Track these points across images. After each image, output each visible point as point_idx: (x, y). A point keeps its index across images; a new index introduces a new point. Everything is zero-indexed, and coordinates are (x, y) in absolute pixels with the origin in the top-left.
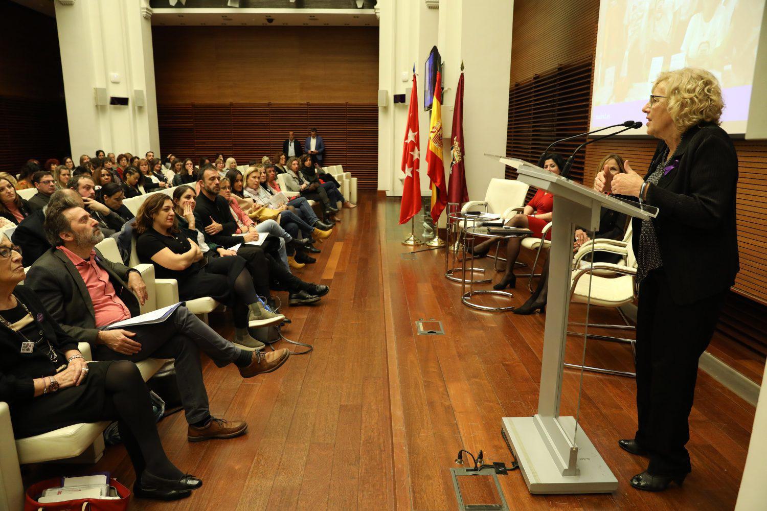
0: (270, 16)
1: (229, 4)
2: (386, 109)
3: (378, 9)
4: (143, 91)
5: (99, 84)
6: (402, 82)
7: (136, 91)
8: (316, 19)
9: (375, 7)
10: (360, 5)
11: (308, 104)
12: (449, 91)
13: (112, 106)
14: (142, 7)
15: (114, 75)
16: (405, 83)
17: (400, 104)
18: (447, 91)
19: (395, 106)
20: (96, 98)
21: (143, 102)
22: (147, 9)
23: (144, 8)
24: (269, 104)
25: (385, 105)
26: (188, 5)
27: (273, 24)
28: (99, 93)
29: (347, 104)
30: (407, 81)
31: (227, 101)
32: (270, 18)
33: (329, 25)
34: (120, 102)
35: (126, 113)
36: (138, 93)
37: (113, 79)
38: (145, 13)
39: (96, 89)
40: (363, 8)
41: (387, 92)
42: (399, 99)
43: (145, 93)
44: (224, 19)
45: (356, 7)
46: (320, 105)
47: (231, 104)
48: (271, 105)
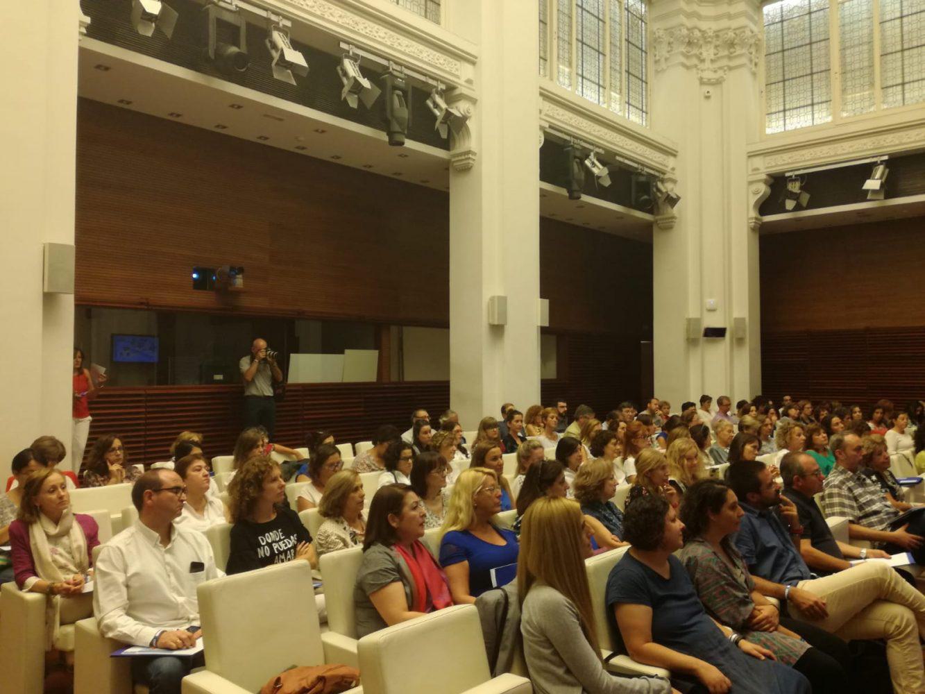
1: (869, 197)
4: (743, 319)
5: (693, 313)
7: (735, 319)
13: (705, 338)
14: (750, 216)
15: (710, 302)
20: (688, 330)
21: (744, 331)
22: (756, 219)
23: (752, 218)
26: (810, 206)
28: (692, 323)
31: (862, 325)
34: (716, 333)
35: (723, 346)
36: (739, 321)
37: (708, 306)
38: (753, 224)
39: (689, 320)
43: (747, 320)
47: (867, 330)
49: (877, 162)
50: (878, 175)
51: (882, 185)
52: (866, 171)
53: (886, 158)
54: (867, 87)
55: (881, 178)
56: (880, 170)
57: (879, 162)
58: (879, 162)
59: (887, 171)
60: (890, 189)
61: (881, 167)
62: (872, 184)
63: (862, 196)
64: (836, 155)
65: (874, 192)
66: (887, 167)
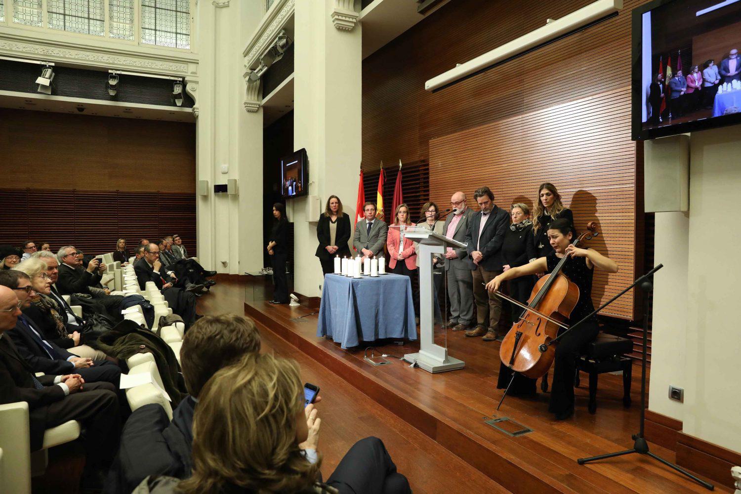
0: (82, 106)
1: (39, 90)
2: (205, 198)
3: (198, 109)
6: (222, 174)
8: (132, 112)
9: (194, 106)
10: (179, 102)
11: (117, 192)
12: (313, 183)
16: (224, 175)
17: (220, 193)
18: (311, 184)
19: (215, 195)
24: (74, 191)
25: (206, 194)
27: (84, 113)
29: (158, 193)
30: (226, 173)
31: (23, 186)
32: (81, 107)
33: (120, 116)
40: (182, 106)
41: (207, 182)
42: (221, 189)
44: (29, 104)
45: (175, 105)
46: (135, 193)
47: (28, 190)
48: (76, 192)
49: (46, 65)
50: (48, 75)
51: (51, 83)
52: (37, 70)
53: (53, 64)
54: (35, 6)
55: (50, 78)
56: (49, 72)
57: (47, 66)
58: (47, 66)
59: (54, 74)
60: (54, 88)
61: (50, 71)
62: (41, 81)
63: (34, 88)
64: (11, 50)
65: (44, 87)
66: (53, 71)
